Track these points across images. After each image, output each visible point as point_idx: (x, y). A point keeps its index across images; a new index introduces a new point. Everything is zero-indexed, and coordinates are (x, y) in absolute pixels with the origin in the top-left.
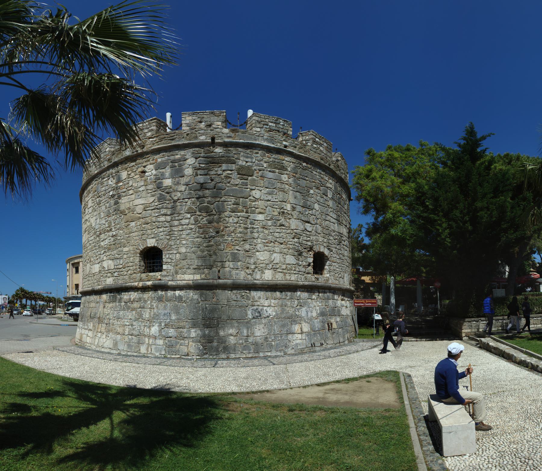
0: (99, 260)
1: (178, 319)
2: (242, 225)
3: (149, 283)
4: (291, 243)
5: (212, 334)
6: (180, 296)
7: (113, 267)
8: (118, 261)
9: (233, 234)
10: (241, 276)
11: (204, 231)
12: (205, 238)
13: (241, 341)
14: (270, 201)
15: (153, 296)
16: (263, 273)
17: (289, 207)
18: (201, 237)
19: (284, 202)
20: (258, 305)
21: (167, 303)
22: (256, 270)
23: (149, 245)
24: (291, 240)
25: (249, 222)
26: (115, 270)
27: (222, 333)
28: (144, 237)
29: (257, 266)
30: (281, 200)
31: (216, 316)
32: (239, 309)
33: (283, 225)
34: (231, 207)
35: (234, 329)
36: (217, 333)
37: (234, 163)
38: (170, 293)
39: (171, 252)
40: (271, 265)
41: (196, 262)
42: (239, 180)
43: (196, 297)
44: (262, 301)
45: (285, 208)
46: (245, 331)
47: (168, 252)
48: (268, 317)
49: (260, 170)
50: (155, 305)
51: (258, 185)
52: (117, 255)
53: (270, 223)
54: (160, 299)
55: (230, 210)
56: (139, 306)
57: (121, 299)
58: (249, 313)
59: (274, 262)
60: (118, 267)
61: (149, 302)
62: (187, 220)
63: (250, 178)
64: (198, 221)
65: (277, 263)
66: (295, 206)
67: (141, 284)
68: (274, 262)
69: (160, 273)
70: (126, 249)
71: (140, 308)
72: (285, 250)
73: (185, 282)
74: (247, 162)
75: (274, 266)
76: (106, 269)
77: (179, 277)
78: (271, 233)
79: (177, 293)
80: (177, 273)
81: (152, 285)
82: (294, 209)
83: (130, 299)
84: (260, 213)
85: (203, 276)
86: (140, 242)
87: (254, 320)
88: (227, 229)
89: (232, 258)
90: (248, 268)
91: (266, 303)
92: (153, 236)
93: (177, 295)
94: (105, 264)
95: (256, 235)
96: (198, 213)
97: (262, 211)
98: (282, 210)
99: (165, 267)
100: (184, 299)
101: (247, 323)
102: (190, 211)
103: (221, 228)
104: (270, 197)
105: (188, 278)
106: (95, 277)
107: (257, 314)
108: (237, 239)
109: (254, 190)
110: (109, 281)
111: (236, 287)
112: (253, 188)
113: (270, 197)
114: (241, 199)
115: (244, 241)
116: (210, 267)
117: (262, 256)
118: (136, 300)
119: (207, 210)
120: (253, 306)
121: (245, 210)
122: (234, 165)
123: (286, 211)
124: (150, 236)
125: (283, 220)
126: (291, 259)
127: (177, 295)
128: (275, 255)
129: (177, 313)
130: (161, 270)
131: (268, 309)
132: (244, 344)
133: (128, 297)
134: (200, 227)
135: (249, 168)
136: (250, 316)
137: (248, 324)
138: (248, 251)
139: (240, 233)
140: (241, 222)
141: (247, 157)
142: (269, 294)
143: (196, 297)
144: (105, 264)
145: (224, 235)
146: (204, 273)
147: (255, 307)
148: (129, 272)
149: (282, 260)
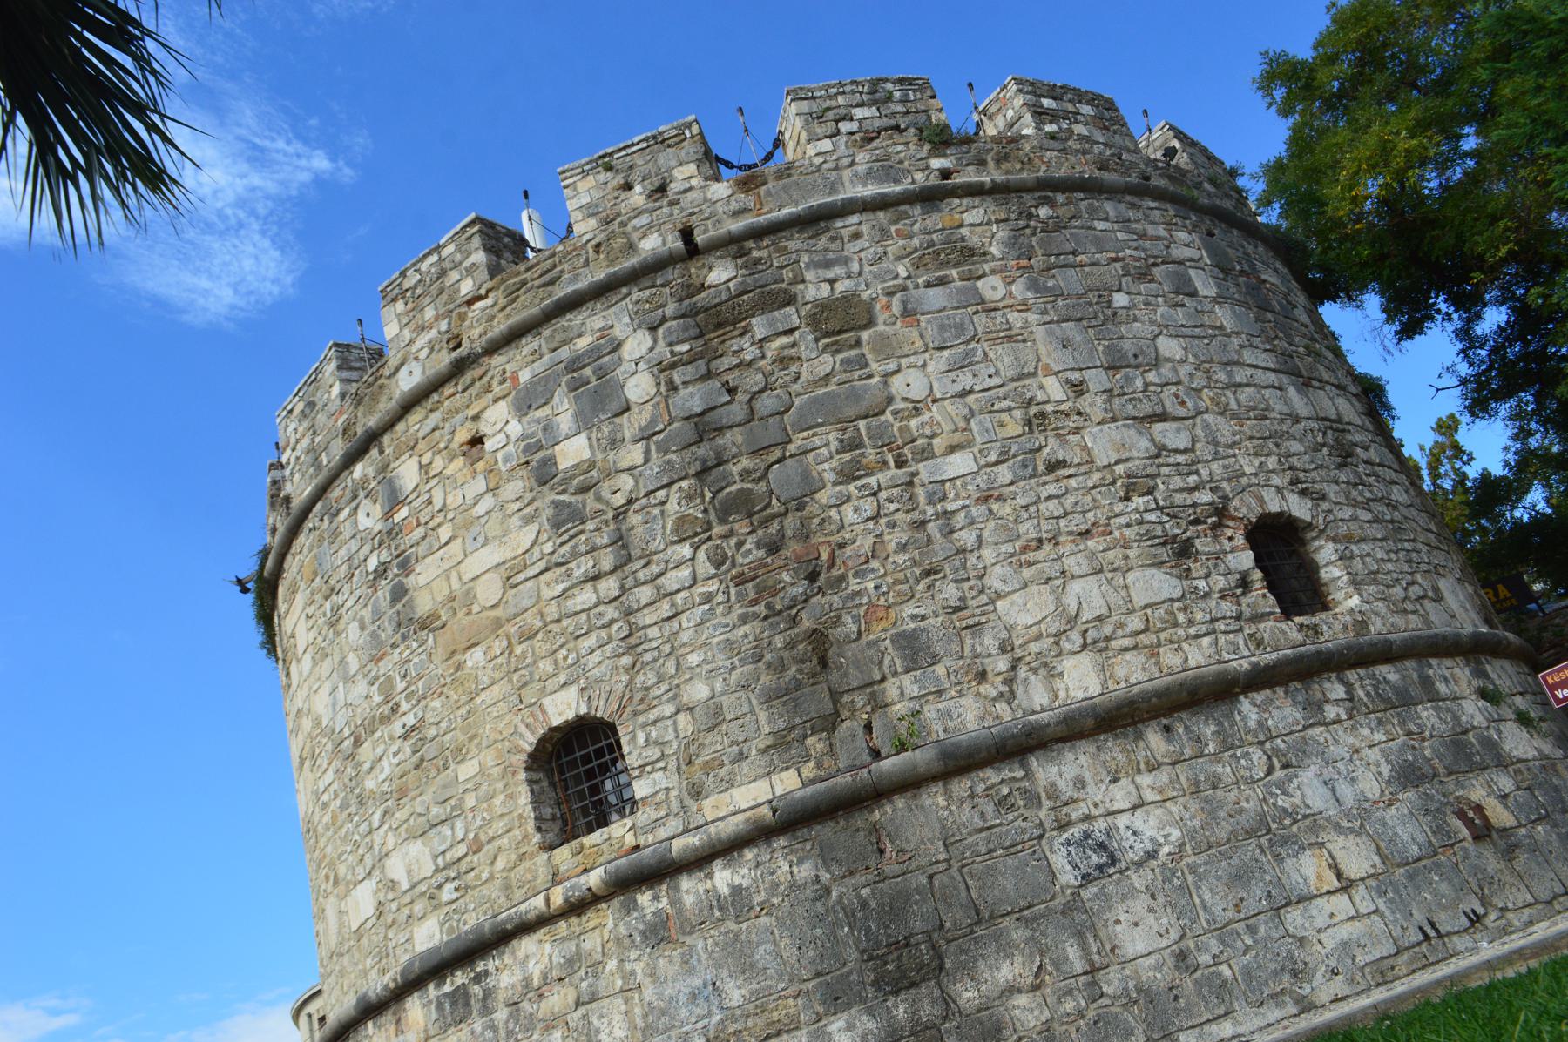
0: (368, 862)
1: (756, 996)
2: (898, 516)
3: (594, 879)
4: (1123, 520)
5: (928, 1011)
6: (736, 890)
7: (428, 869)
8: (446, 830)
9: (874, 564)
10: (969, 716)
11: (760, 590)
12: (773, 612)
13: (1069, 1005)
14: (971, 392)
15: (623, 930)
16: (1053, 674)
17: (1054, 390)
18: (756, 616)
19: (1030, 375)
20: (1087, 818)
21: (689, 940)
22: (1022, 672)
23: (556, 721)
24: (1119, 507)
25: (922, 499)
26: (440, 878)
27: (968, 995)
28: (530, 696)
29: (1019, 653)
30: (1011, 373)
31: (918, 925)
32: (1010, 862)
33: (1063, 464)
34: (834, 463)
35: (1018, 959)
36: (947, 1000)
37: (790, 300)
38: (690, 888)
39: (652, 716)
40: (1075, 636)
41: (765, 722)
42: (827, 358)
43: (805, 871)
44: (1095, 793)
45: (1041, 396)
46: (1073, 953)
47: (641, 719)
48: (1151, 855)
49: (891, 294)
50: (639, 968)
51: (906, 350)
52: (435, 810)
53: (1004, 473)
54: (657, 934)
55: (833, 477)
56: (571, 999)
57: (488, 994)
58: (1059, 860)
59: (1085, 616)
60: (448, 856)
61: (612, 964)
62: (684, 567)
63: (865, 335)
64: (725, 557)
65: (1099, 618)
66: (1075, 376)
67: (558, 898)
68: (1085, 616)
69: (628, 822)
70: (467, 770)
71: (578, 1004)
72: (1111, 555)
73: (741, 817)
74: (832, 282)
75: (1091, 635)
76: (405, 886)
77: (712, 806)
78: (1025, 507)
79: (723, 877)
80: (697, 792)
81: (606, 883)
82: (1078, 388)
83: (527, 981)
84: (952, 449)
85: (809, 770)
86: (517, 720)
87: (1093, 890)
88: (848, 551)
89: (904, 658)
90: (982, 676)
91: (1120, 796)
92: (562, 679)
93: (724, 890)
94: (396, 868)
95: (967, 537)
96: (718, 530)
97: (957, 438)
98: (1034, 410)
99: (640, 789)
100: (757, 899)
101: (1067, 910)
102: (685, 531)
103: (825, 556)
104: (966, 380)
105: (751, 795)
106: (364, 941)
107: (1095, 859)
108: (900, 576)
109: (897, 372)
110: (428, 936)
111: (961, 762)
112: (892, 366)
113: (966, 380)
114: (862, 424)
115: (928, 573)
116: (829, 723)
117: (1024, 611)
118: (555, 974)
119: (742, 505)
120: (1062, 826)
121: (890, 459)
122: (791, 310)
123: (1049, 408)
124: (551, 685)
125: (1053, 442)
127: (724, 890)
128: (1076, 587)
129: (747, 968)
130: (628, 805)
131: (1138, 820)
132: (1091, 1014)
133: (518, 976)
134: (741, 580)
135: (849, 299)
136: (1068, 877)
137: (1078, 917)
138: (957, 609)
139: (903, 548)
140: (893, 507)
141: (828, 264)
142: (1114, 750)
143: (805, 871)
144: (396, 868)
145: (842, 578)
146: (807, 757)
147: (1076, 831)
148: (500, 864)
149: (1116, 599)
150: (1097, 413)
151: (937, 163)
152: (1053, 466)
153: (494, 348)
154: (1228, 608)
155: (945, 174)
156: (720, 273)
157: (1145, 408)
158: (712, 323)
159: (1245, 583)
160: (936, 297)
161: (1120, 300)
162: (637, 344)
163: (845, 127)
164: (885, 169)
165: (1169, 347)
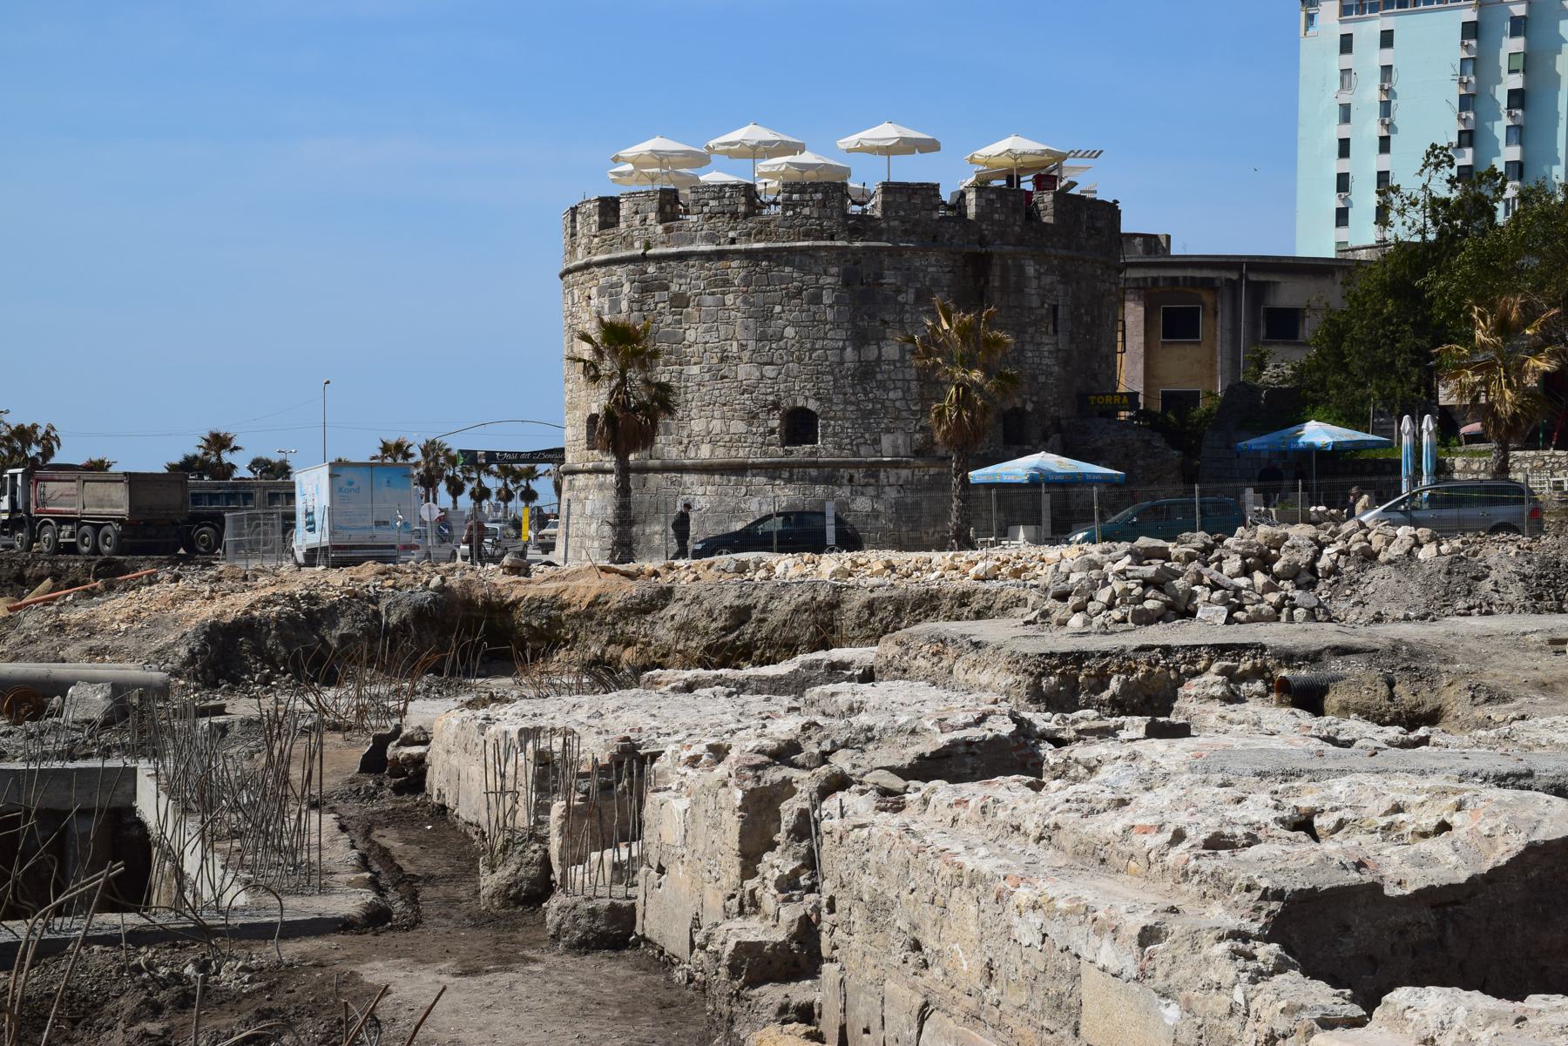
44: (695, 488)
67: (590, 465)
82: (743, 347)
91: (700, 490)
95: (689, 396)
117: (697, 426)
126: (738, 427)
141: (680, 277)
142: (705, 477)
150: (745, 359)
151: (731, 234)
152: (723, 377)
153: (600, 264)
154: (760, 440)
155: (733, 241)
156: (651, 269)
157: (765, 359)
158: (647, 288)
159: (772, 431)
160: (709, 300)
161: (778, 309)
162: (626, 288)
163: (706, 209)
164: (711, 238)
165: (790, 332)
